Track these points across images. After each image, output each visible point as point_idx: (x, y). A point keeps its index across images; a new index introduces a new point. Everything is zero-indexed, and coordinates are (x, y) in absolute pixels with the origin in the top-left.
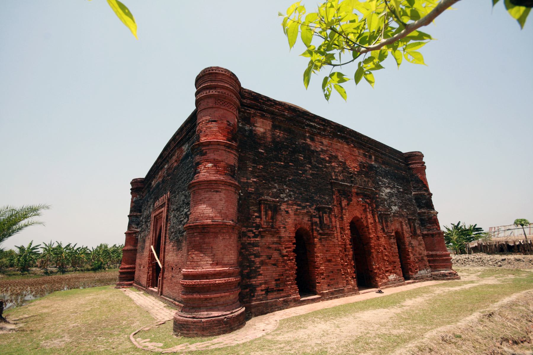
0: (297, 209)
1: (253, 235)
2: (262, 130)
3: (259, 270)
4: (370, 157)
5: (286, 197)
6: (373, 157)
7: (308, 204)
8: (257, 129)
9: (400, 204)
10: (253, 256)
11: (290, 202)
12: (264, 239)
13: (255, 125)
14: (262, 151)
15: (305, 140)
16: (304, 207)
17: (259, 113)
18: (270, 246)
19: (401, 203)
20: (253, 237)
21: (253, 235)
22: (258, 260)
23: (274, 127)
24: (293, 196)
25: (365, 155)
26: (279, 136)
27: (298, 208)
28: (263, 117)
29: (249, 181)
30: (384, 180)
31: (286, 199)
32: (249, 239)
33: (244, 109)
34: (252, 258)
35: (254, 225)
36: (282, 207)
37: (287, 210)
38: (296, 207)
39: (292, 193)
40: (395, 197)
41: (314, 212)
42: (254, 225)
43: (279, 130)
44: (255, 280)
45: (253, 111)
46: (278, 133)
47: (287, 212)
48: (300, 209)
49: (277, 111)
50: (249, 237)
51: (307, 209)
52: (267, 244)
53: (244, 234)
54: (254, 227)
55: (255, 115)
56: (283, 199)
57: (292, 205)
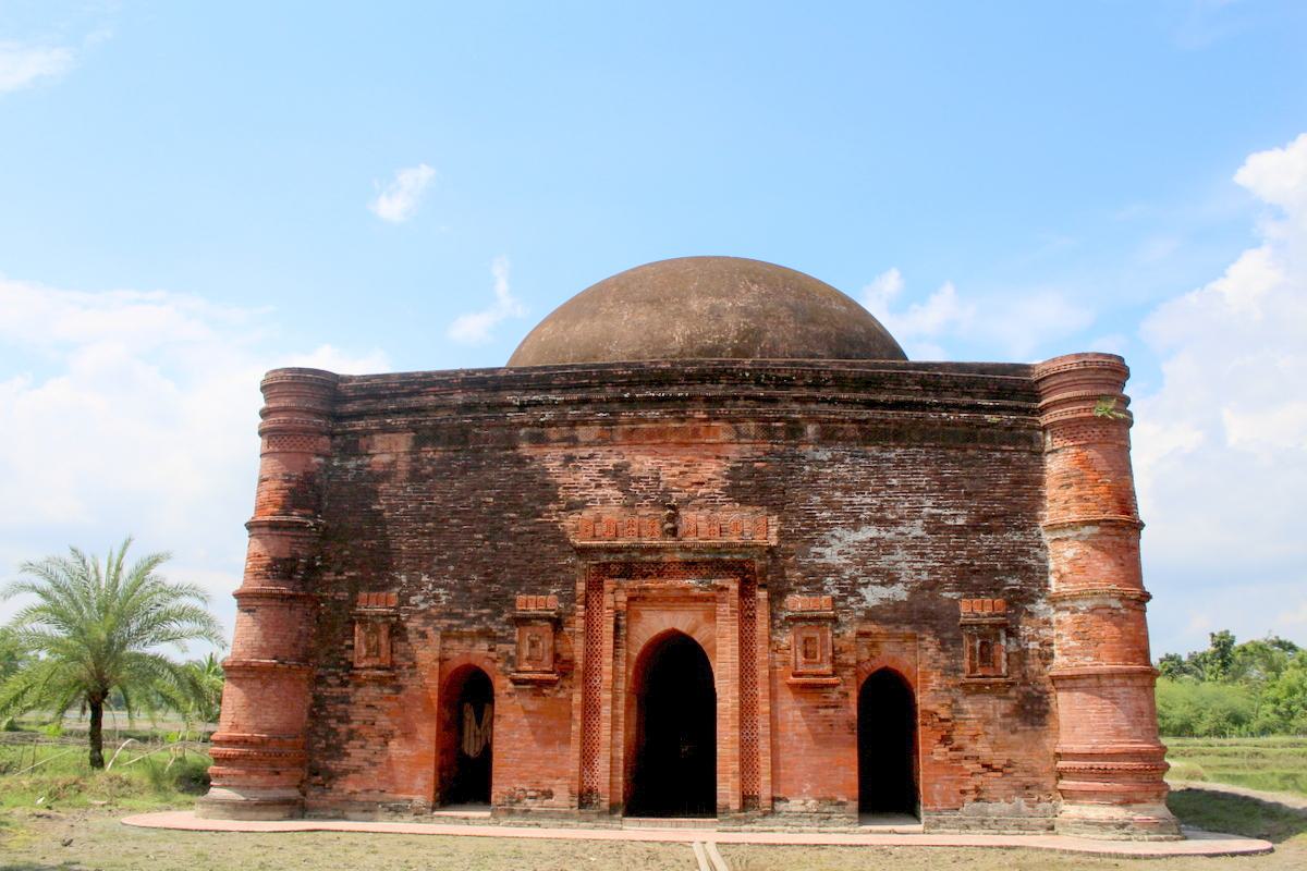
0: (450, 626)
1: (338, 682)
2: (386, 458)
3: (345, 746)
4: (794, 430)
5: (423, 601)
6: (811, 429)
7: (484, 611)
8: (374, 459)
9: (925, 576)
10: (335, 721)
11: (433, 611)
12: (361, 690)
13: (371, 452)
14: (378, 507)
15: (513, 449)
16: (473, 621)
17: (376, 424)
18: (373, 703)
19: (932, 571)
20: (338, 686)
21: (338, 682)
22: (343, 728)
23: (420, 442)
24: (444, 598)
25: (770, 434)
26: (432, 460)
27: (456, 622)
28: (386, 429)
29: (339, 578)
30: (857, 499)
31: (422, 606)
32: (329, 689)
33: (341, 426)
34: (333, 723)
35: (342, 663)
36: (409, 625)
37: (422, 629)
38: (449, 622)
39: (441, 591)
40: (900, 554)
41: (503, 630)
42: (342, 663)
43: (434, 445)
44: (337, 762)
45: (360, 425)
46: (430, 453)
47: (423, 635)
48: (459, 626)
49: (432, 397)
50: (330, 686)
51: (482, 623)
52: (367, 699)
53: (320, 680)
54: (341, 666)
55: (368, 433)
56: (416, 605)
57: (439, 616)
